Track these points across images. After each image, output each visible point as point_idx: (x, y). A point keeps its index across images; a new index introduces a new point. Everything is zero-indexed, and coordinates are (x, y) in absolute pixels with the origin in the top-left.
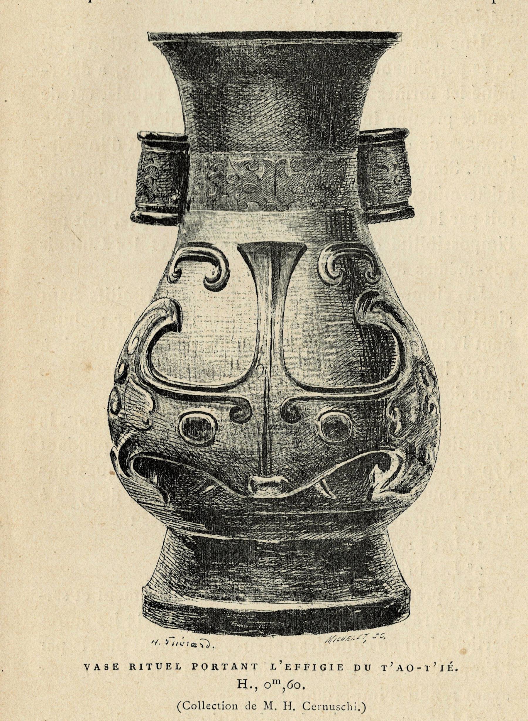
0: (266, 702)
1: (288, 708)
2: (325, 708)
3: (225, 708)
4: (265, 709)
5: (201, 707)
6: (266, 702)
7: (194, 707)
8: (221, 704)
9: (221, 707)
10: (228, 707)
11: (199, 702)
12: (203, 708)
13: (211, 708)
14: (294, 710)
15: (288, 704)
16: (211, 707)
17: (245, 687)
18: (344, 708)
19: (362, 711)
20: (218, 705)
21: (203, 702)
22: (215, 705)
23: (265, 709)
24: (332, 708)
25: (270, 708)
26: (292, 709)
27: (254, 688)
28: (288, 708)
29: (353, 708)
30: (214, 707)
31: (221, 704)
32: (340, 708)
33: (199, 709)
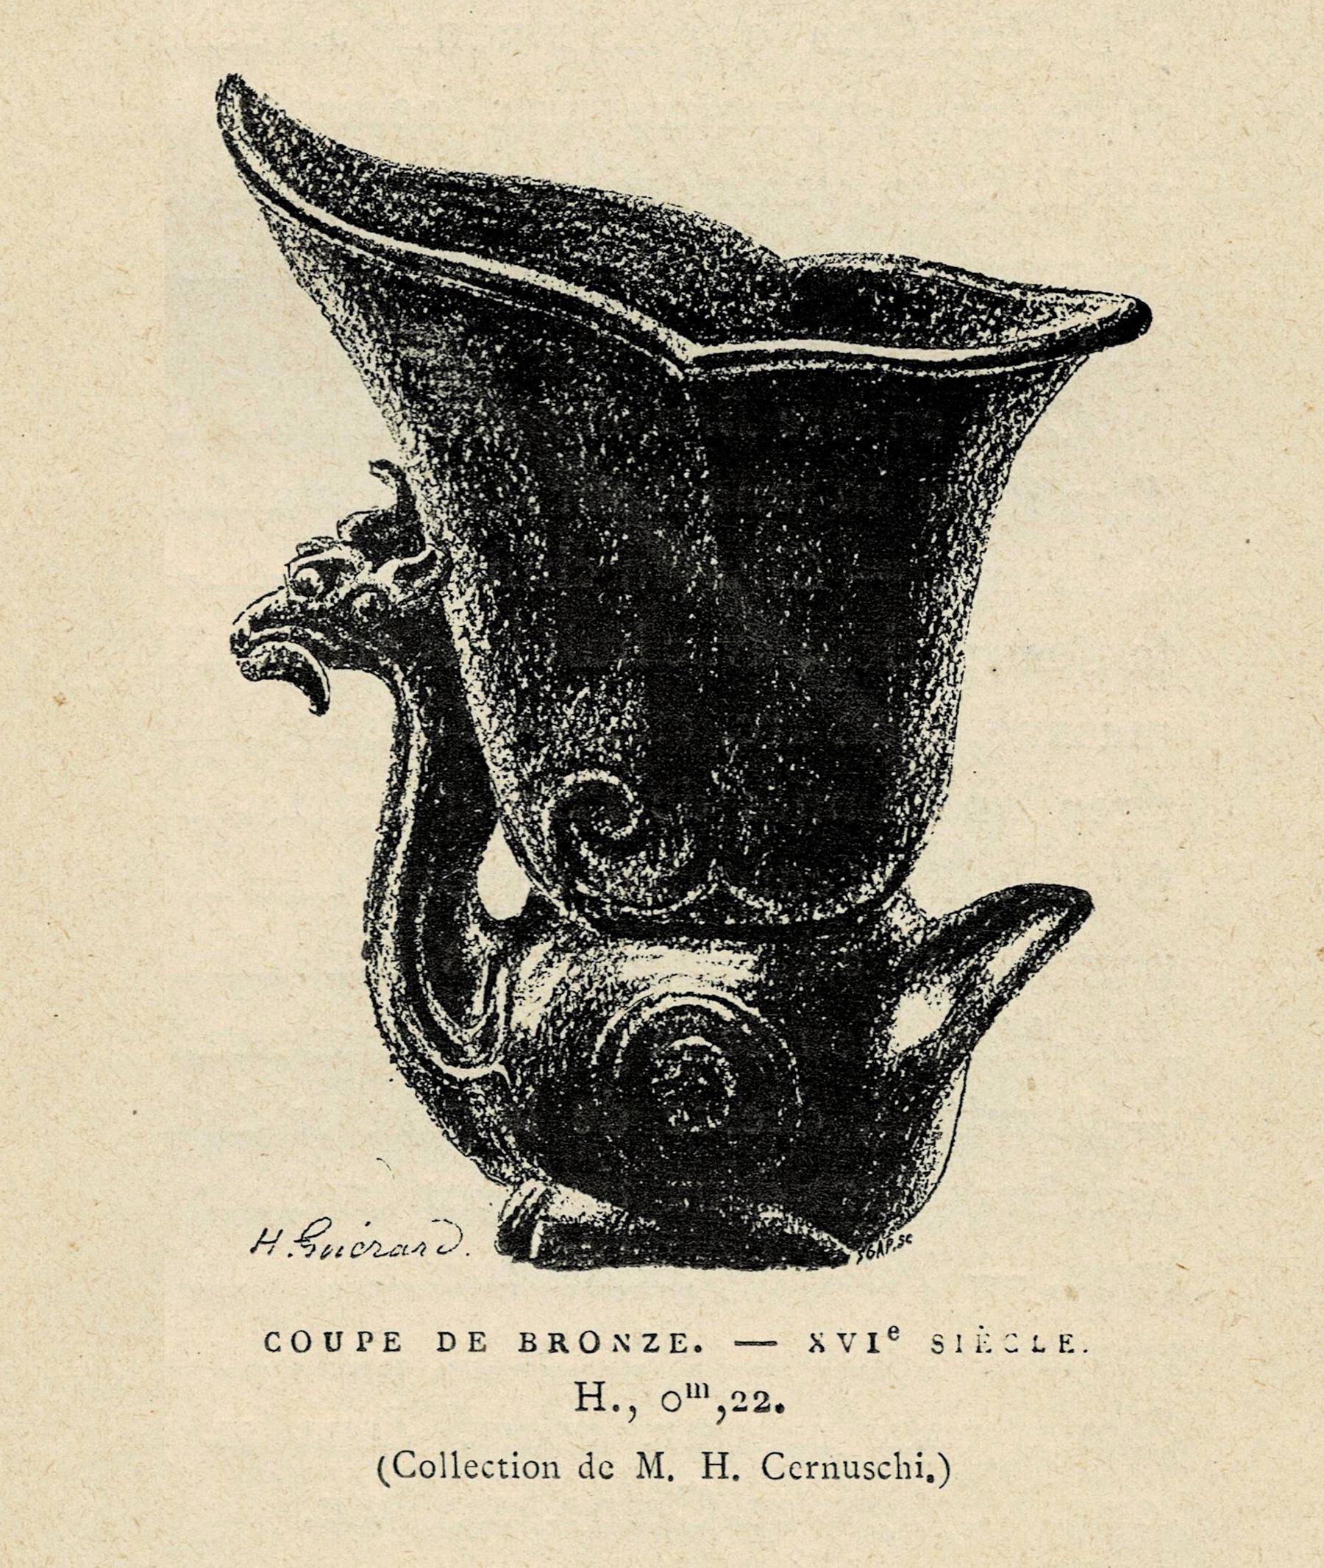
0: (642, 1454)
1: (716, 1471)
2: (830, 1470)
3: (520, 1473)
4: (641, 1476)
6: (642, 1454)
7: (427, 1469)
9: (508, 1470)
10: (531, 1469)
11: (442, 1454)
12: (456, 1476)
13: (480, 1474)
14: (736, 1477)
15: (715, 1458)
16: (478, 1470)
18: (884, 1470)
19: (939, 1480)
20: (501, 1463)
22: (490, 1462)
23: (641, 1476)
24: (851, 1471)
25: (654, 1473)
27: (609, 1409)
28: (716, 1471)
29: (914, 1470)
30: (489, 1469)
31: (510, 1459)
32: (875, 1469)
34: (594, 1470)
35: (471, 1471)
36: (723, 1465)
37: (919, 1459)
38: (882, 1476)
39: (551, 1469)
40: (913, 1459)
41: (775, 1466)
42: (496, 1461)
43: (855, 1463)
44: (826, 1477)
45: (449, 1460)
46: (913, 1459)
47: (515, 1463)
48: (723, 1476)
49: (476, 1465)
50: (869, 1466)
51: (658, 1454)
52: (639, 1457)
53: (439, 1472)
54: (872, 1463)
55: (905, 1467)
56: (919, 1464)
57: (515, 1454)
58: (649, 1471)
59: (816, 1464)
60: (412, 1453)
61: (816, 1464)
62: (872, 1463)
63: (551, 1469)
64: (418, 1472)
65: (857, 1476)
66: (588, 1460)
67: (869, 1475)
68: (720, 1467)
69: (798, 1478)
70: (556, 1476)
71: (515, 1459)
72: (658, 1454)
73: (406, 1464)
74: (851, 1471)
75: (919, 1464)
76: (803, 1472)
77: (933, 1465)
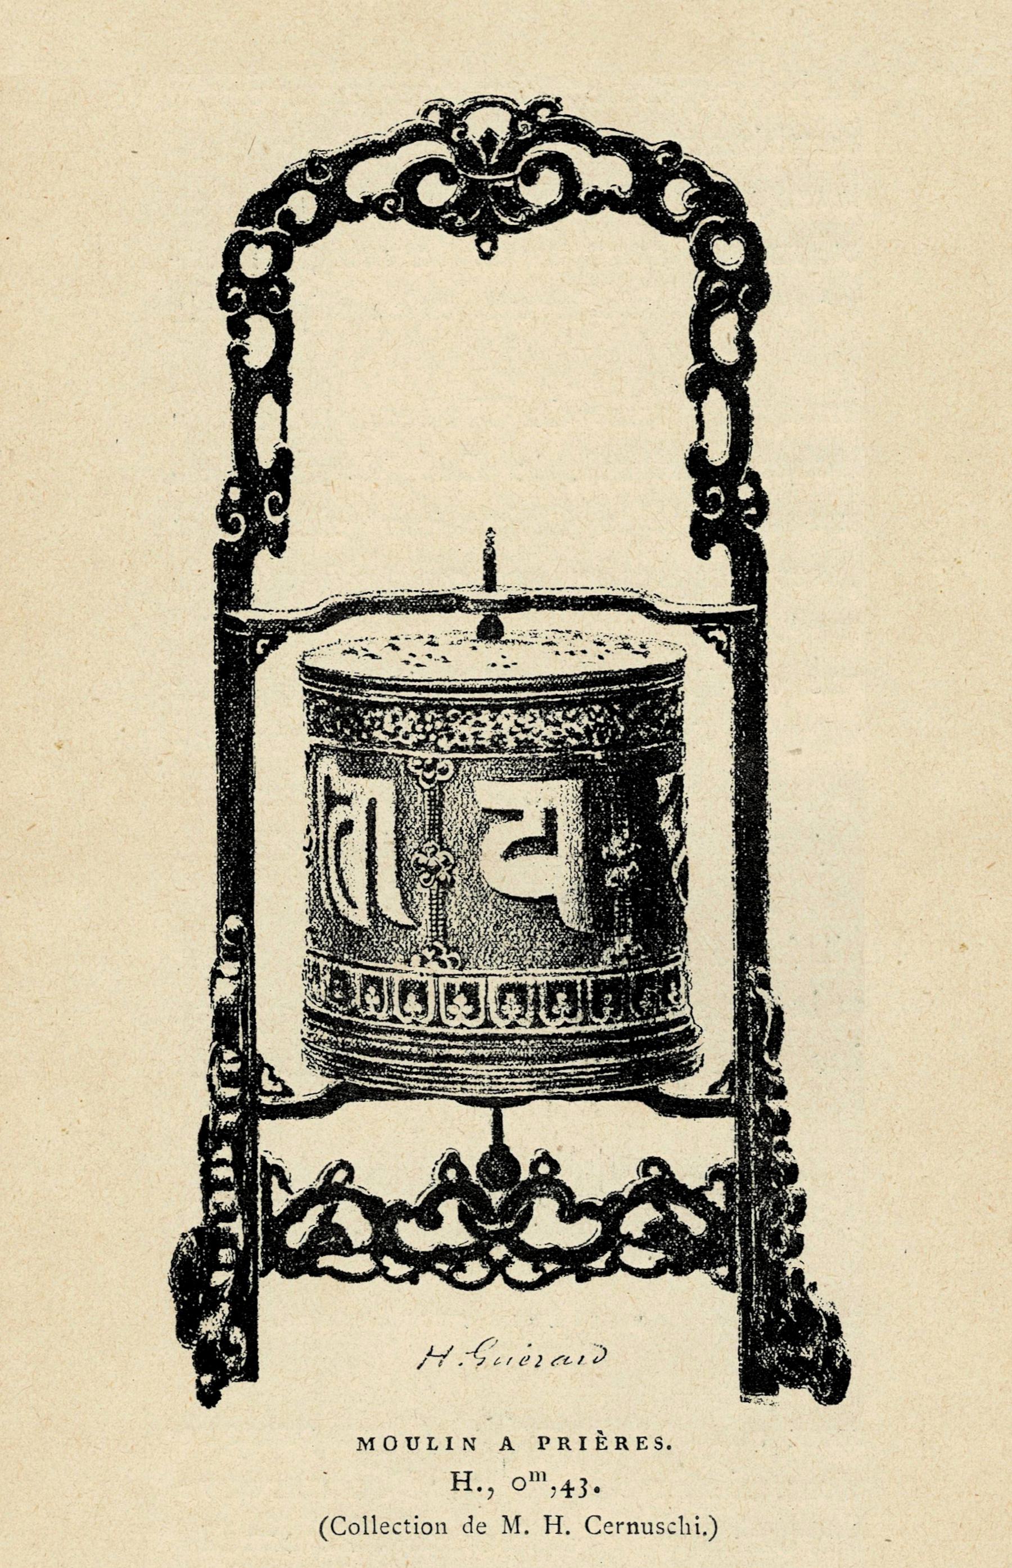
0: (506, 1517)
1: (553, 1529)
2: (633, 1528)
3: (419, 1530)
5: (370, 1530)
6: (506, 1517)
7: (354, 1529)
8: (412, 1521)
9: (411, 1528)
10: (427, 1529)
11: (365, 1517)
12: (375, 1532)
14: (568, 1533)
15: (553, 1520)
16: (390, 1529)
17: (468, 1489)
18: (672, 1528)
19: (710, 1535)
20: (406, 1523)
21: (374, 1517)
22: (400, 1524)
24: (647, 1530)
25: (514, 1530)
26: (563, 1530)
28: (553, 1529)
29: (693, 1529)
30: (398, 1528)
31: (412, 1521)
32: (665, 1527)
33: (366, 1533)
34: (473, 1526)
35: (385, 1530)
36: (559, 1524)
37: (697, 1521)
38: (671, 1533)
39: (441, 1527)
40: (693, 1522)
41: (594, 1525)
42: (403, 1522)
43: (650, 1524)
44: (630, 1533)
45: (370, 1519)
46: (693, 1522)
47: (416, 1524)
48: (559, 1532)
49: (388, 1526)
50: (660, 1525)
51: (517, 1518)
52: (504, 1519)
53: (362, 1529)
54: (663, 1523)
55: (687, 1526)
56: (697, 1525)
57: (416, 1517)
58: (511, 1529)
59: (622, 1523)
60: (344, 1518)
61: (622, 1523)
62: (663, 1523)
63: (441, 1527)
64: (348, 1532)
65: (651, 1533)
66: (470, 1521)
67: (661, 1531)
68: (557, 1526)
69: (611, 1533)
70: (445, 1532)
71: (416, 1521)
72: (517, 1518)
73: (340, 1526)
74: (647, 1530)
75: (697, 1525)
76: (614, 1529)
77: (707, 1526)
